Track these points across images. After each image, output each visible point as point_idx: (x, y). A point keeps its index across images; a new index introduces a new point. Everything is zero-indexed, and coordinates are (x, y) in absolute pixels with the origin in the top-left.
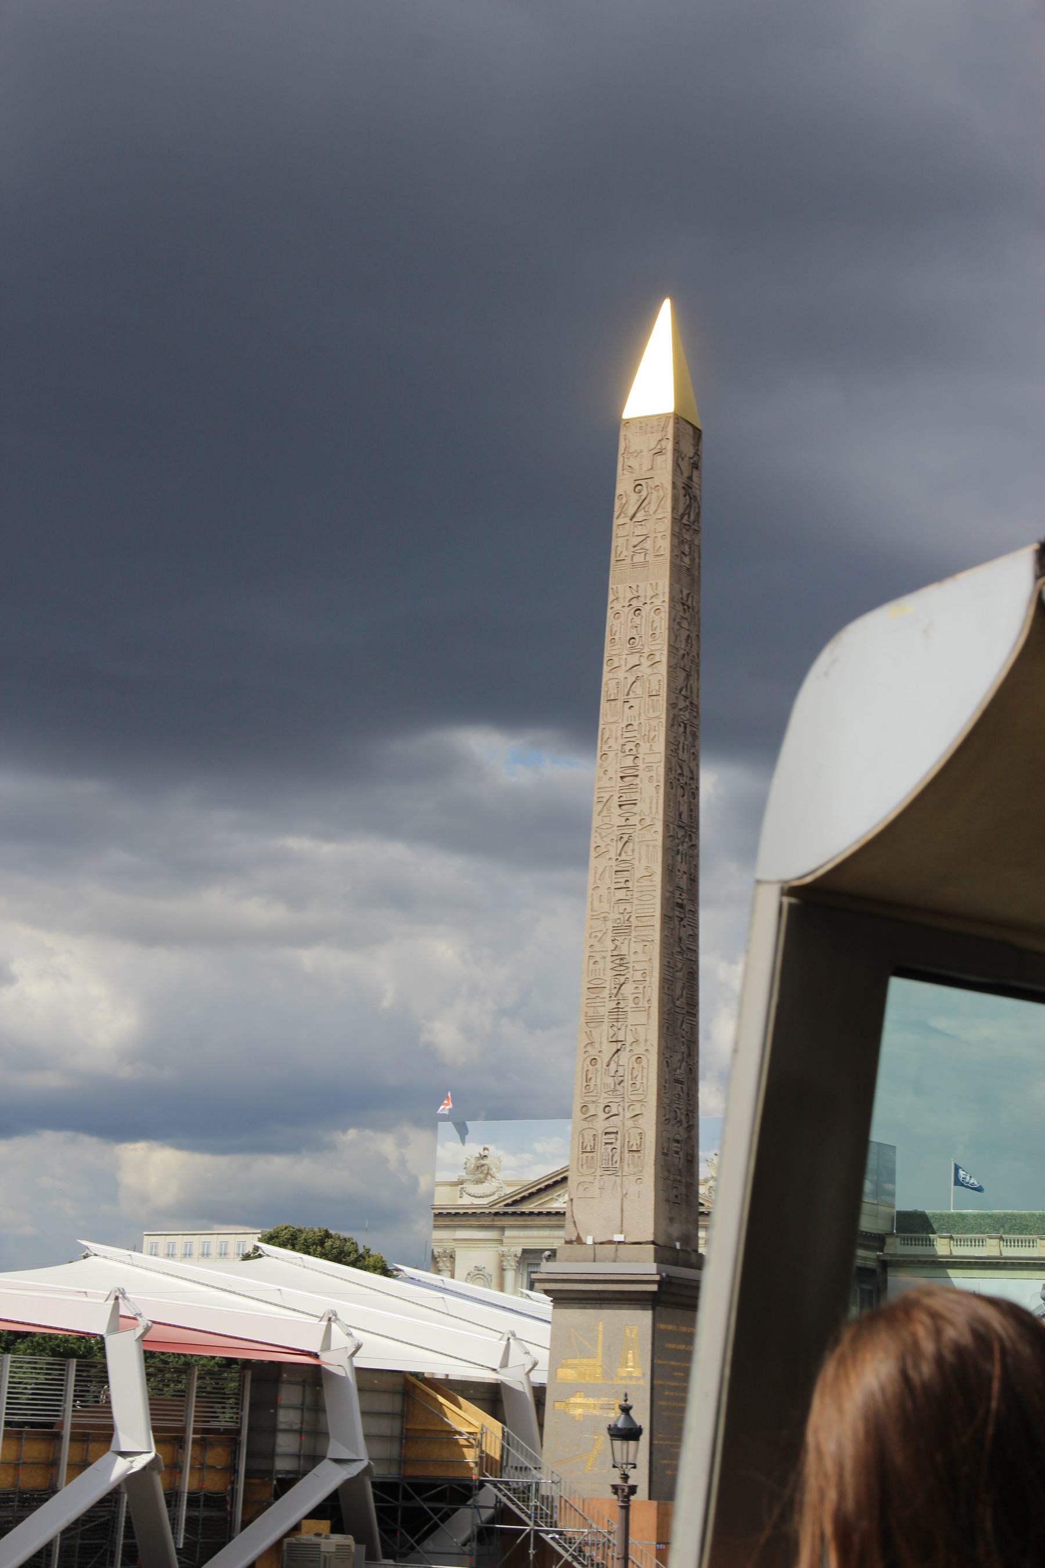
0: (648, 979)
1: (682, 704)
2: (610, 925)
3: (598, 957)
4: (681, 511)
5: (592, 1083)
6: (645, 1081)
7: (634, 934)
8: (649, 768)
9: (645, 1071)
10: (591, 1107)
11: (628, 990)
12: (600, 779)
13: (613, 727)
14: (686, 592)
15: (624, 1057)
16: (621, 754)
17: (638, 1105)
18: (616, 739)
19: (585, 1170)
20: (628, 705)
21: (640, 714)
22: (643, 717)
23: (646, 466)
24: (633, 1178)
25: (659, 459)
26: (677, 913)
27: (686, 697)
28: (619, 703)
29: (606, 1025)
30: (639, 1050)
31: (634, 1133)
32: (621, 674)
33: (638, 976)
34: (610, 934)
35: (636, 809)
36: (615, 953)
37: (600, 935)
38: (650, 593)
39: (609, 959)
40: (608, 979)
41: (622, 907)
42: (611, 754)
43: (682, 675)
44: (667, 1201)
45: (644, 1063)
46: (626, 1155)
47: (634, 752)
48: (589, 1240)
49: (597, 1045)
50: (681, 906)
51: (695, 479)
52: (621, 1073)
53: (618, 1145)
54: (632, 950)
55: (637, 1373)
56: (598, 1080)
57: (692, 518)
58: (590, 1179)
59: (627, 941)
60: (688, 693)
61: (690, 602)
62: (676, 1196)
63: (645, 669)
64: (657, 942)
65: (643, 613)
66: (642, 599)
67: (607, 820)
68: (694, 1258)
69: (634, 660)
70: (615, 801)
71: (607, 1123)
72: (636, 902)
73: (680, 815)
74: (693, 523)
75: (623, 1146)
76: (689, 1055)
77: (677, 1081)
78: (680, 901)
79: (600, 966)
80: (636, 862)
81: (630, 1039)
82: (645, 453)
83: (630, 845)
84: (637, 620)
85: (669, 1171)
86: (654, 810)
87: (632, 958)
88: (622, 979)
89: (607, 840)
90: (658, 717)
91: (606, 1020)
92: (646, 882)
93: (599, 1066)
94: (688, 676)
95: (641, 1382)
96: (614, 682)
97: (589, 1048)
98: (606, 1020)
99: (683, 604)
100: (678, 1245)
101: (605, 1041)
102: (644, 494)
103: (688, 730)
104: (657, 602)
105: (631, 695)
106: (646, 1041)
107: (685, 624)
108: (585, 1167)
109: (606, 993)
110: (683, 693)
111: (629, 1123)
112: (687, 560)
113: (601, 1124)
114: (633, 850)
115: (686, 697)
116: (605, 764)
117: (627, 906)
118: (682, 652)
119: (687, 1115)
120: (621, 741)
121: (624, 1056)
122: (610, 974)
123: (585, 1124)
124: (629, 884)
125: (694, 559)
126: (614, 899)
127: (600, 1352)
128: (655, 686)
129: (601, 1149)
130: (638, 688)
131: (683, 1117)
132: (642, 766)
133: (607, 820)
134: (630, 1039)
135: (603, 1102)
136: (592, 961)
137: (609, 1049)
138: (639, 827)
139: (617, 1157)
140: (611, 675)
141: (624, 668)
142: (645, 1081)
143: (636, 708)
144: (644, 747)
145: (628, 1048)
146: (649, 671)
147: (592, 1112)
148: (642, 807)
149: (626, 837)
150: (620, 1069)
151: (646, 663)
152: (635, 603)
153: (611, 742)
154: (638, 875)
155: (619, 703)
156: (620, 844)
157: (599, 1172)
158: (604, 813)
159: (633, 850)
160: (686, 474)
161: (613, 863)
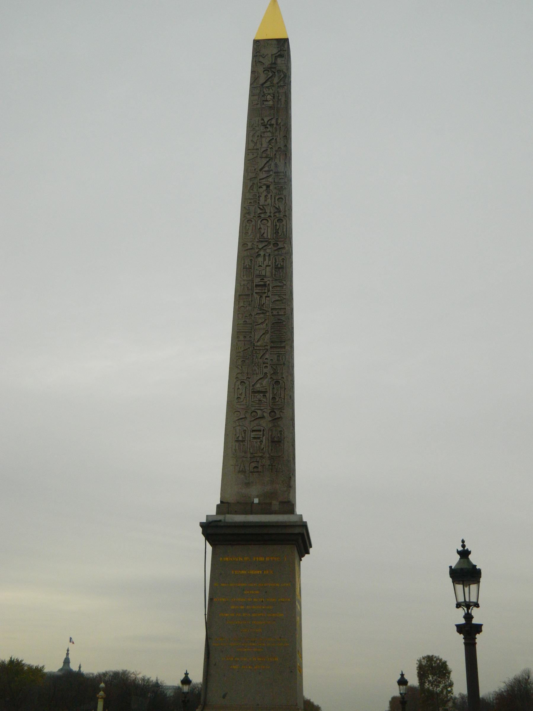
1: (264, 175)
14: (266, 120)
27: (269, 171)
43: (264, 161)
50: (265, 285)
60: (273, 167)
61: (273, 122)
74: (277, 83)
76: (275, 373)
77: (259, 392)
85: (246, 452)
100: (256, 501)
103: (271, 187)
110: (266, 169)
118: (263, 149)
125: (279, 100)
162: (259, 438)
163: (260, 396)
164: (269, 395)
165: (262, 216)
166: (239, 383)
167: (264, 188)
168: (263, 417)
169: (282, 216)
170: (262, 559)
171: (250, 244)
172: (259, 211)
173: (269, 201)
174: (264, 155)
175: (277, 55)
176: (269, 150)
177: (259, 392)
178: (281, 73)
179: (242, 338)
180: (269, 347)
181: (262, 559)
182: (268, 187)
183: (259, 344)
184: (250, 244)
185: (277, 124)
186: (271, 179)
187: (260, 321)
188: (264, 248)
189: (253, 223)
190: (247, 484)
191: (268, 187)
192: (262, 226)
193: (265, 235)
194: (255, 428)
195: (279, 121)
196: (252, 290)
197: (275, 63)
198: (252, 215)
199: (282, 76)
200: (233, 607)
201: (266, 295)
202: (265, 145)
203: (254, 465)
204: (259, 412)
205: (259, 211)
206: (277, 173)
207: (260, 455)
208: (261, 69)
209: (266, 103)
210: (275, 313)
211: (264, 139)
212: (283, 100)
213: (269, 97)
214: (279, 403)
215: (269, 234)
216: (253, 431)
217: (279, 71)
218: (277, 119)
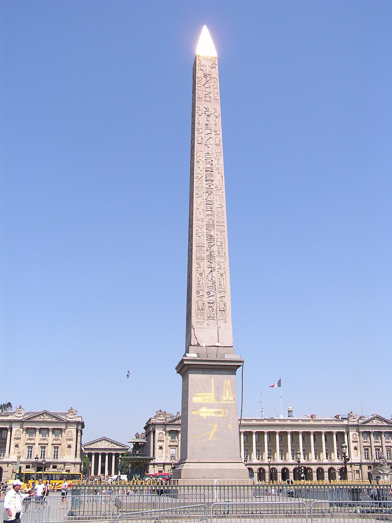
0: (223, 245)
5: (201, 283)
6: (225, 284)
7: (215, 228)
9: (225, 280)
11: (215, 248)
15: (215, 274)
17: (223, 293)
18: (203, 157)
21: (212, 151)
25: (213, 69)
28: (203, 145)
29: (206, 261)
30: (222, 271)
33: (219, 244)
35: (213, 183)
36: (208, 234)
39: (205, 236)
40: (206, 244)
41: (210, 217)
45: (224, 277)
46: (218, 312)
47: (211, 163)
48: (204, 345)
49: (202, 268)
53: (215, 308)
54: (215, 234)
55: (231, 398)
56: (204, 281)
58: (203, 321)
59: (213, 231)
67: (201, 185)
69: (209, 131)
70: (204, 179)
75: (217, 308)
80: (215, 202)
81: (217, 267)
82: (207, 66)
83: (211, 196)
86: (221, 184)
87: (216, 237)
88: (212, 244)
91: (205, 259)
95: (234, 402)
96: (200, 138)
97: (198, 269)
98: (205, 259)
101: (206, 267)
102: (208, 78)
105: (208, 143)
106: (224, 268)
108: (199, 316)
109: (205, 249)
114: (213, 198)
117: (212, 217)
120: (205, 158)
122: (206, 242)
123: (199, 299)
127: (213, 389)
129: (206, 309)
132: (214, 168)
133: (201, 185)
134: (217, 267)
135: (206, 290)
136: (197, 236)
139: (214, 312)
142: (225, 284)
144: (215, 162)
145: (216, 271)
146: (215, 136)
147: (201, 294)
149: (210, 192)
153: (200, 158)
155: (203, 145)
156: (207, 194)
157: (206, 318)
158: (199, 182)
159: (213, 198)
161: (205, 201)
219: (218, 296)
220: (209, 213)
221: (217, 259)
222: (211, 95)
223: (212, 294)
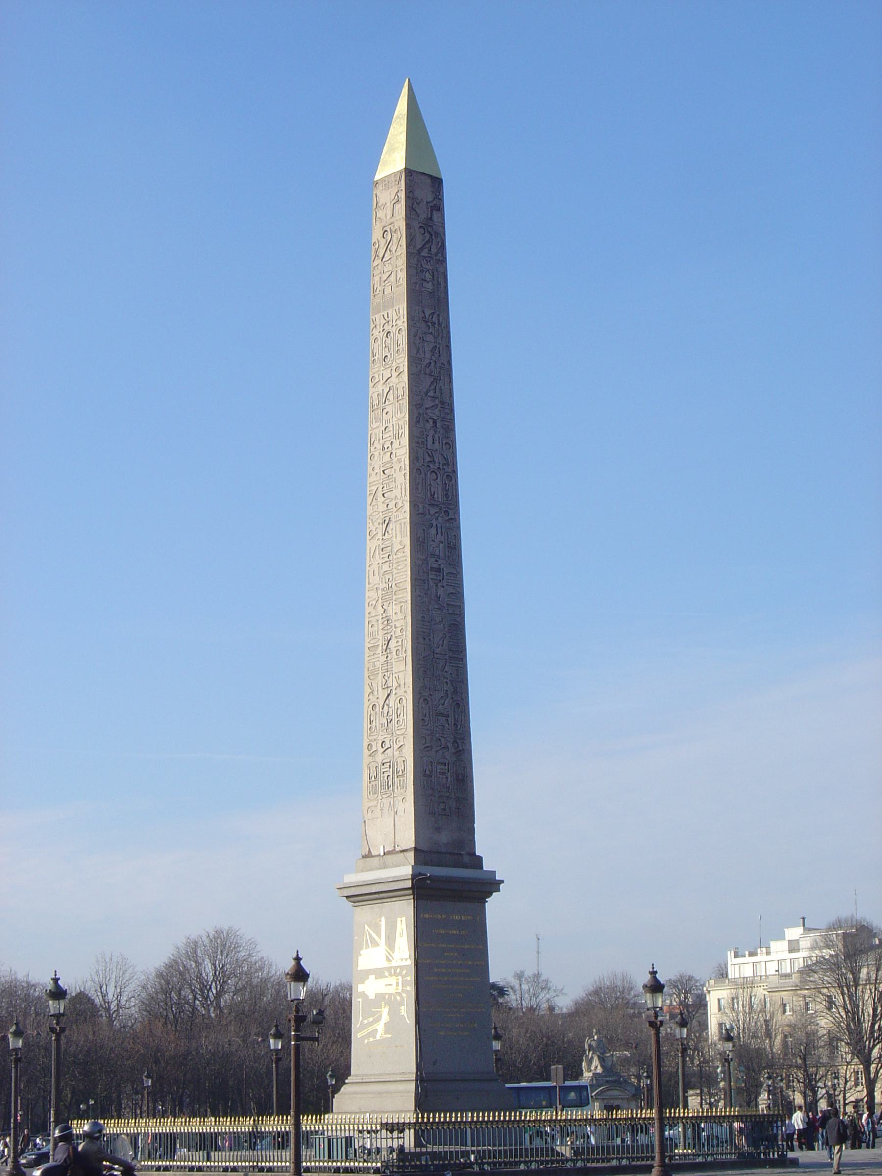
1: (429, 403)
2: (380, 592)
3: (374, 620)
4: (419, 246)
7: (395, 597)
8: (399, 461)
10: (374, 744)
11: (393, 644)
12: (371, 475)
13: (377, 431)
14: (428, 312)
16: (382, 453)
19: (372, 796)
20: (385, 411)
22: (394, 419)
23: (389, 214)
24: (400, 798)
25: (397, 206)
26: (431, 577)
27: (434, 398)
29: (380, 675)
31: (400, 760)
32: (380, 387)
34: (380, 600)
37: (374, 603)
38: (395, 317)
42: (376, 454)
44: (432, 813)
49: (376, 693)
50: (438, 570)
51: (435, 218)
52: (390, 713)
53: (391, 774)
57: (434, 250)
62: (444, 809)
63: (394, 379)
64: (409, 602)
65: (392, 334)
66: (390, 323)
68: (466, 859)
71: (383, 756)
72: (395, 571)
73: (433, 496)
74: (436, 254)
75: (393, 773)
76: (455, 692)
77: (442, 715)
78: (435, 566)
79: (375, 628)
81: (395, 684)
82: (388, 204)
83: (390, 525)
84: (388, 341)
85: (433, 789)
89: (376, 524)
90: (404, 417)
92: (400, 554)
93: (377, 710)
94: (436, 380)
96: (376, 395)
99: (426, 322)
101: (380, 689)
104: (400, 323)
107: (430, 338)
110: (431, 394)
111: (397, 753)
112: (429, 286)
113: (380, 758)
115: (434, 398)
116: (373, 462)
118: (428, 361)
119: (455, 742)
120: (382, 441)
121: (392, 697)
124: (391, 557)
125: (439, 284)
126: (382, 572)
128: (401, 393)
130: (390, 397)
131: (450, 745)
132: (395, 459)
135: (381, 739)
137: (383, 695)
138: (395, 509)
140: (374, 390)
141: (382, 382)
143: (390, 413)
144: (396, 445)
148: (397, 492)
150: (390, 710)
151: (395, 374)
152: (387, 328)
154: (395, 550)
155: (380, 411)
156: (384, 526)
160: (423, 216)
161: (380, 542)
162: (444, 773)
163: (443, 720)
164: (451, 720)
165: (431, 465)
166: (422, 701)
167: (431, 421)
168: (446, 747)
169: (450, 470)
170: (458, 918)
171: (421, 506)
172: (428, 459)
173: (436, 443)
174: (428, 371)
175: (432, 204)
176: (433, 364)
177: (442, 715)
178: (439, 239)
179: (422, 640)
180: (447, 657)
181: (458, 918)
182: (435, 422)
183: (437, 651)
184: (421, 506)
185: (439, 325)
186: (437, 412)
187: (438, 619)
188: (437, 515)
189: (423, 475)
190: (438, 829)
191: (435, 422)
192: (432, 482)
193: (436, 496)
194: (441, 761)
195: (441, 321)
196: (427, 573)
197: (431, 218)
198: (421, 460)
199: (440, 244)
200: (435, 970)
201: (439, 584)
202: (428, 355)
203: (442, 806)
204: (443, 740)
205: (428, 459)
206: (442, 403)
207: (447, 794)
208: (416, 225)
209: (425, 284)
210: (451, 611)
211: (426, 344)
212: (443, 285)
213: (428, 276)
214: (460, 732)
215: (439, 496)
216: (439, 763)
217: (437, 234)
218: (438, 315)
219: (396, 747)
220: (385, 567)
221: (395, 670)
222: (392, 278)
223: (388, 746)
